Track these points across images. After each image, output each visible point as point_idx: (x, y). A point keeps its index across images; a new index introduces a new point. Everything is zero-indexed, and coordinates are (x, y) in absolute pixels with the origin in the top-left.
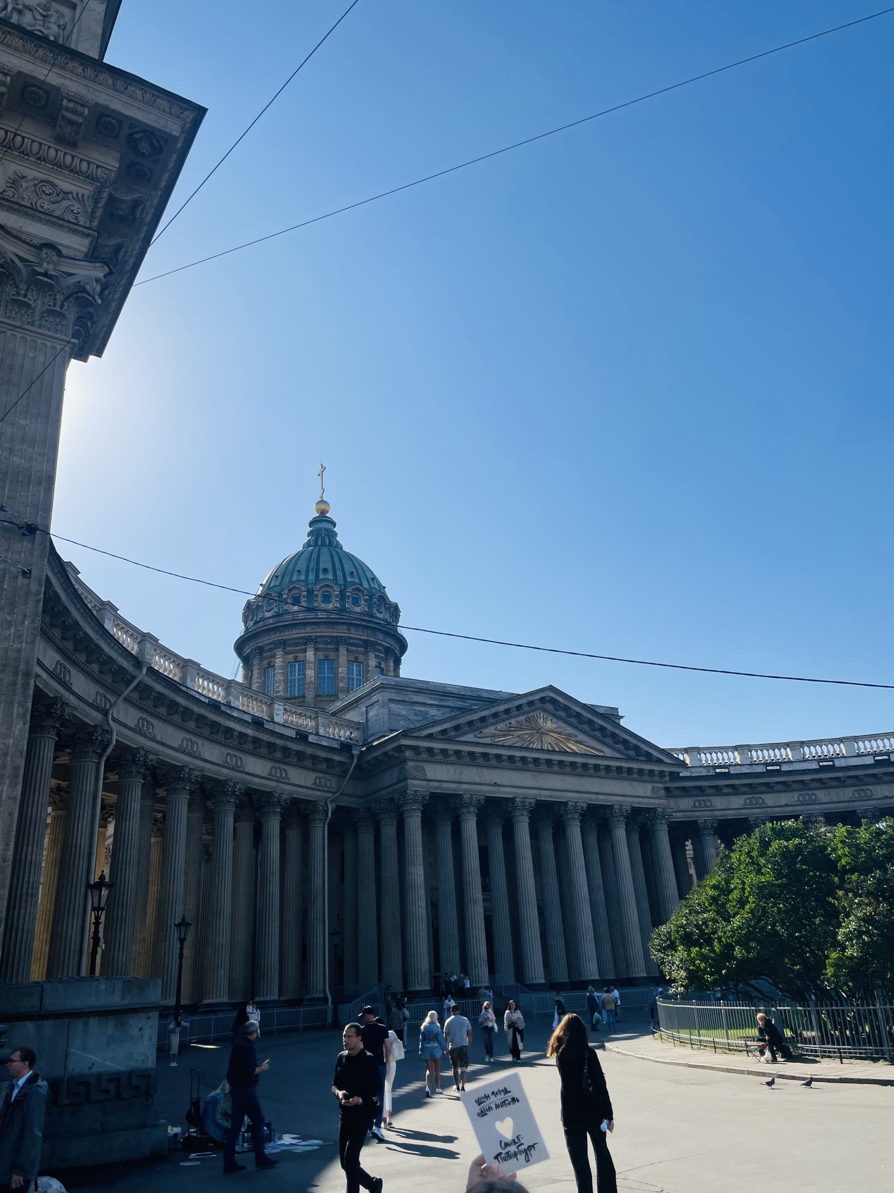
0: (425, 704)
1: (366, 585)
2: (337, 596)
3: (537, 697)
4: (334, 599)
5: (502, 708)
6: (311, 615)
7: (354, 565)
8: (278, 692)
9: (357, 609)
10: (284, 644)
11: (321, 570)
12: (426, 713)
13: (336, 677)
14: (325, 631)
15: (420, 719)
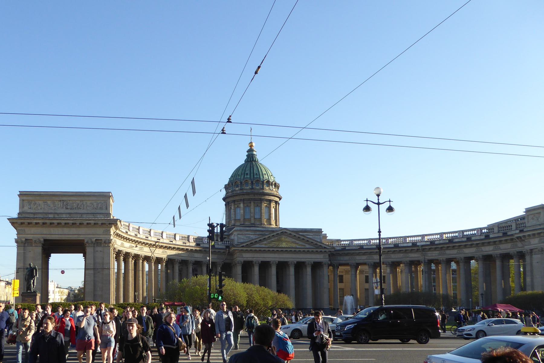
0: (249, 234)
1: (261, 177)
2: (250, 184)
3: (280, 232)
4: (249, 185)
5: (267, 237)
6: (242, 191)
7: (258, 170)
8: (232, 218)
9: (258, 188)
10: (234, 201)
11: (246, 174)
12: (250, 237)
13: (251, 213)
14: (246, 197)
15: (247, 238)
